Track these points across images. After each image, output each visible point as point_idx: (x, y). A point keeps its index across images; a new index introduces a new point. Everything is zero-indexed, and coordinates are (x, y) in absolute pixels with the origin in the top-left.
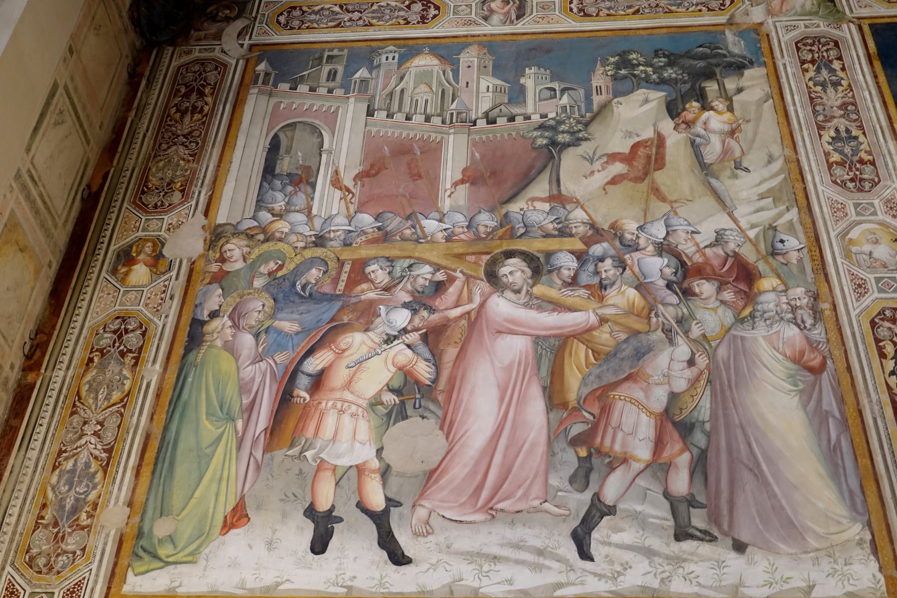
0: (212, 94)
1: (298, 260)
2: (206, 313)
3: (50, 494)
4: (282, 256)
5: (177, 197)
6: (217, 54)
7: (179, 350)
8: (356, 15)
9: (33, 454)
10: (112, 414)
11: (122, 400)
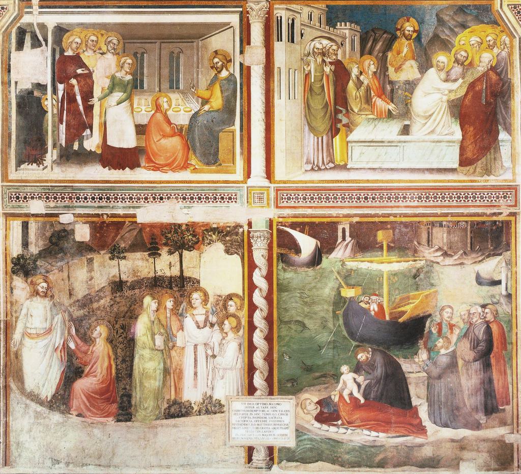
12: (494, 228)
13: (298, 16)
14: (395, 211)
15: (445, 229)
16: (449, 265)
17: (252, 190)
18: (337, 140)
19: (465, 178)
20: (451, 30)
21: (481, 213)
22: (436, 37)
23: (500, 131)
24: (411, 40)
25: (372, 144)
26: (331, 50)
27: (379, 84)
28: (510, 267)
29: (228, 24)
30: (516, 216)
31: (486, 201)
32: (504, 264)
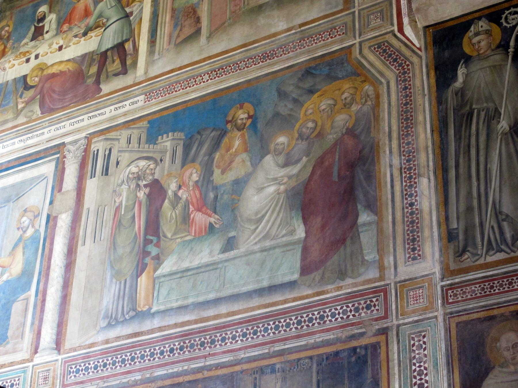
12: (353, 359)
13: (116, 143)
14: (210, 362)
15: (278, 374)
17: (38, 369)
18: (143, 280)
19: (310, 292)
20: (295, 101)
21: (333, 339)
23: (360, 213)
24: (245, 130)
25: (185, 274)
26: (148, 171)
29: (43, 175)
30: (387, 334)
31: (339, 319)
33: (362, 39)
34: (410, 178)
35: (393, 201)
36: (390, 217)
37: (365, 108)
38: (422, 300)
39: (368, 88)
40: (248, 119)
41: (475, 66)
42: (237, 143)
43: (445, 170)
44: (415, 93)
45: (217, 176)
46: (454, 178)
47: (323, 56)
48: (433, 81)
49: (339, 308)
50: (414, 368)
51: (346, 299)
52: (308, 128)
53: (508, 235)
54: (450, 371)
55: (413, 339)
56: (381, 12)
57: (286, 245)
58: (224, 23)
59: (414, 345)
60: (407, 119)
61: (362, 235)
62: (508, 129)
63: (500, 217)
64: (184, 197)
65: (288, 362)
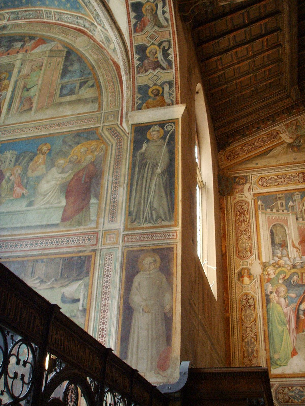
0: (248, 214)
1: (290, 273)
2: (269, 292)
3: (244, 349)
4: (285, 273)
5: (249, 253)
6: (244, 198)
7: (265, 305)
8: (283, 180)
9: (236, 337)
10: (253, 325)
11: (254, 321)
12: (79, 261)
14: (14, 254)
15: (45, 263)
16: (44, 289)
19: (64, 229)
22: (61, 150)
27: (21, 181)
28: (87, 288)
31: (75, 243)
32: (83, 287)
33: (104, 125)
34: (116, 187)
35: (107, 196)
36: (104, 202)
37: (100, 154)
38: (113, 240)
39: (103, 146)
40: (47, 150)
41: (151, 144)
42: (41, 160)
43: (132, 185)
44: (123, 151)
45: (29, 173)
46: (135, 189)
47: (85, 129)
48: (132, 147)
49: (76, 238)
50: (105, 268)
51: (80, 234)
52: (74, 159)
53: (154, 217)
54: (121, 271)
55: (107, 255)
56: (114, 115)
57: (56, 208)
58: (43, 107)
59: (107, 258)
60: (118, 162)
61: (91, 208)
62: (161, 172)
63: (152, 209)
64: (13, 180)
65: (50, 258)
